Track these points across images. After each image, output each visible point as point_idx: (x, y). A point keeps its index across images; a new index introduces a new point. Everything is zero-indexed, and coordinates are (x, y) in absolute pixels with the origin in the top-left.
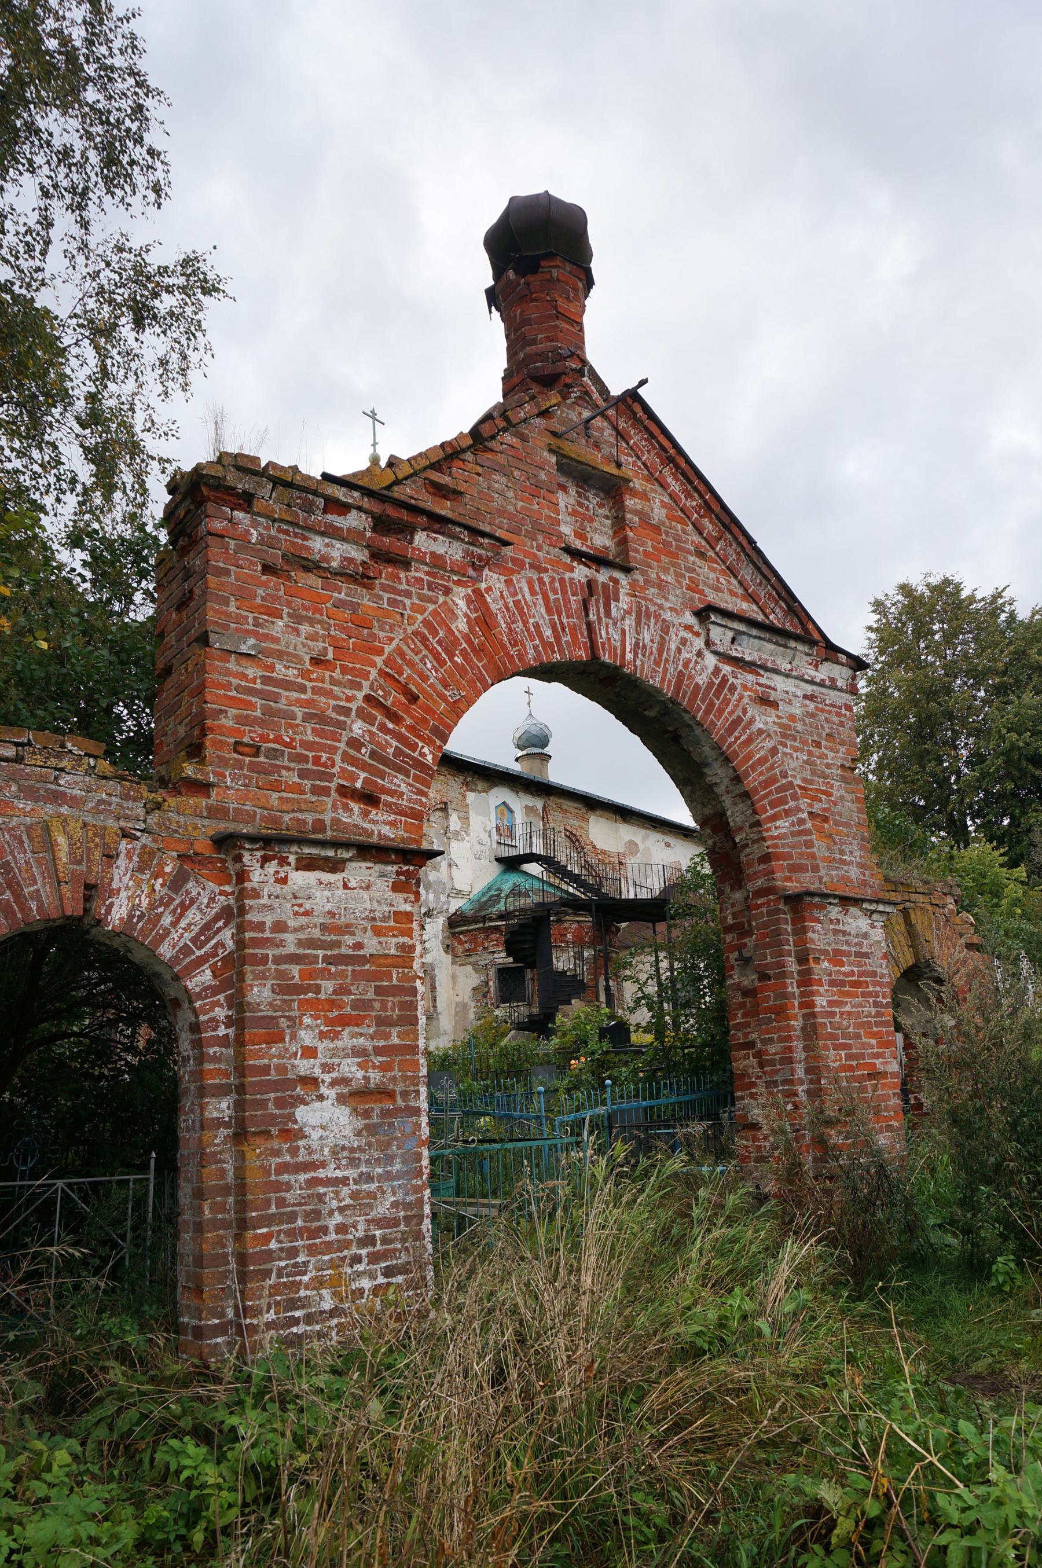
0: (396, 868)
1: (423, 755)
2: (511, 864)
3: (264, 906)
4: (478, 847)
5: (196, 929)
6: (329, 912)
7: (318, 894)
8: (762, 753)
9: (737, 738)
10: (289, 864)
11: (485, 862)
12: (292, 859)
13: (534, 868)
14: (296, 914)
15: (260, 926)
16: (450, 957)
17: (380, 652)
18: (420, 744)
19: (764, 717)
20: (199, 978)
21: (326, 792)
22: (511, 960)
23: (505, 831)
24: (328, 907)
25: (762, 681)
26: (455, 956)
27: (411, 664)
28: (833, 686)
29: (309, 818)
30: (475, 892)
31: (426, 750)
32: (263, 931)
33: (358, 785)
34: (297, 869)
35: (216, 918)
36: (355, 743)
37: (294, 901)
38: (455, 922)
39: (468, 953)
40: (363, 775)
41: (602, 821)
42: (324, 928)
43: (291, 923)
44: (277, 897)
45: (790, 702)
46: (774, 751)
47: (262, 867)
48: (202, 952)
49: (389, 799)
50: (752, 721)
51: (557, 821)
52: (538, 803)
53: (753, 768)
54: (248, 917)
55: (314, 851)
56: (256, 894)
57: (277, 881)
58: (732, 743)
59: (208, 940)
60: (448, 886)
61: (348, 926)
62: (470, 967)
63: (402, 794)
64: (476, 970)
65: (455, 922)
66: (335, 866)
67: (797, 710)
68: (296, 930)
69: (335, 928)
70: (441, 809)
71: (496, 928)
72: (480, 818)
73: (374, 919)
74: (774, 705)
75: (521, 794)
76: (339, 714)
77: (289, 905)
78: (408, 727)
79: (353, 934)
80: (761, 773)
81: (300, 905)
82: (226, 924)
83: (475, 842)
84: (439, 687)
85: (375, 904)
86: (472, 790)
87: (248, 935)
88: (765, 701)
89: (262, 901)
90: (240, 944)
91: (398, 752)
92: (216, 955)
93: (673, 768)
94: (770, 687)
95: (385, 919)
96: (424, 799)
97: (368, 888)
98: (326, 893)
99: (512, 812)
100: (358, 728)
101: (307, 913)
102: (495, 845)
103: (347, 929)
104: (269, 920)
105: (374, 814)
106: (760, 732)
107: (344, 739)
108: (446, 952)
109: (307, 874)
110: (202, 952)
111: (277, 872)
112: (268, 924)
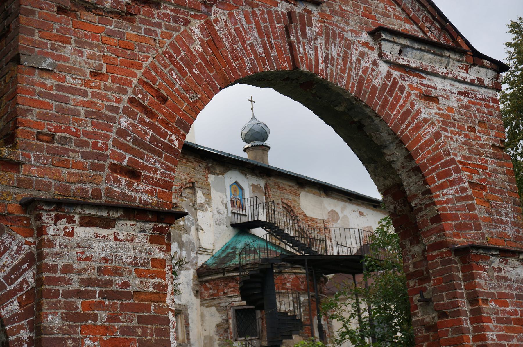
0: (152, 225)
1: (172, 141)
2: (243, 228)
3: (57, 253)
4: (217, 216)
5: (8, 270)
6: (104, 258)
7: (96, 245)
8: (428, 137)
9: (408, 126)
10: (75, 222)
11: (223, 227)
12: (77, 218)
13: (260, 232)
14: (79, 259)
15: (53, 269)
17: (140, 67)
18: (169, 133)
19: (428, 110)
20: (9, 307)
21: (101, 168)
22: (245, 303)
23: (237, 204)
24: (103, 254)
25: (425, 82)
27: (161, 75)
28: (481, 84)
29: (89, 187)
31: (173, 137)
32: (55, 272)
33: (125, 163)
34: (80, 226)
35: (22, 262)
36: (122, 133)
37: (78, 250)
38: (203, 274)
40: (128, 156)
42: (100, 270)
43: (76, 267)
44: (66, 246)
45: (448, 98)
46: (437, 135)
47: (55, 224)
48: (12, 287)
49: (147, 174)
50: (419, 112)
53: (422, 148)
54: (45, 261)
55: (93, 212)
56: (51, 244)
57: (66, 234)
58: (405, 129)
59: (17, 278)
61: (118, 269)
62: (214, 309)
63: (157, 170)
64: (219, 311)
65: (203, 274)
66: (108, 223)
67: (453, 103)
68: (79, 272)
69: (109, 270)
70: (190, 188)
71: (233, 278)
72: (219, 194)
73: (136, 264)
74: (435, 100)
76: (110, 111)
77: (74, 253)
78: (160, 121)
79: (121, 275)
80: (429, 153)
81: (83, 253)
82: (29, 267)
83: (215, 212)
84: (182, 91)
85: (138, 253)
86: (212, 173)
87: (45, 275)
88: (428, 97)
89: (55, 250)
90: (39, 281)
91: (153, 139)
92: (21, 290)
94: (431, 87)
95: (145, 264)
96: (172, 174)
97: (132, 240)
98: (101, 244)
100: (124, 121)
101: (88, 259)
102: (230, 215)
103: (117, 271)
104: (60, 264)
105: (137, 185)
106: (426, 121)
107: (115, 130)
109: (88, 229)
110: (12, 287)
111: (66, 228)
112: (60, 267)
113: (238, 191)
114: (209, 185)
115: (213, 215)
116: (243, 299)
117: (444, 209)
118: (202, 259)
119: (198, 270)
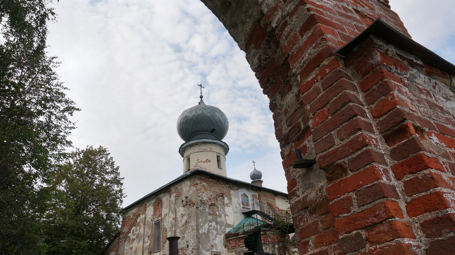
2: (248, 214)
4: (235, 209)
11: (238, 214)
16: (227, 249)
22: (248, 249)
23: (245, 204)
26: (228, 249)
30: (236, 224)
38: (228, 236)
39: (234, 248)
41: (280, 200)
51: (264, 200)
52: (257, 194)
60: (225, 223)
62: (234, 253)
65: (228, 236)
70: (221, 196)
71: (242, 237)
72: (236, 199)
75: (250, 191)
83: (234, 207)
86: (233, 190)
93: (222, 17)
99: (247, 197)
102: (242, 208)
108: (225, 248)
113: (246, 198)
114: (231, 195)
115: (233, 209)
116: (246, 246)
117: (322, 14)
118: (228, 230)
119: (226, 235)
